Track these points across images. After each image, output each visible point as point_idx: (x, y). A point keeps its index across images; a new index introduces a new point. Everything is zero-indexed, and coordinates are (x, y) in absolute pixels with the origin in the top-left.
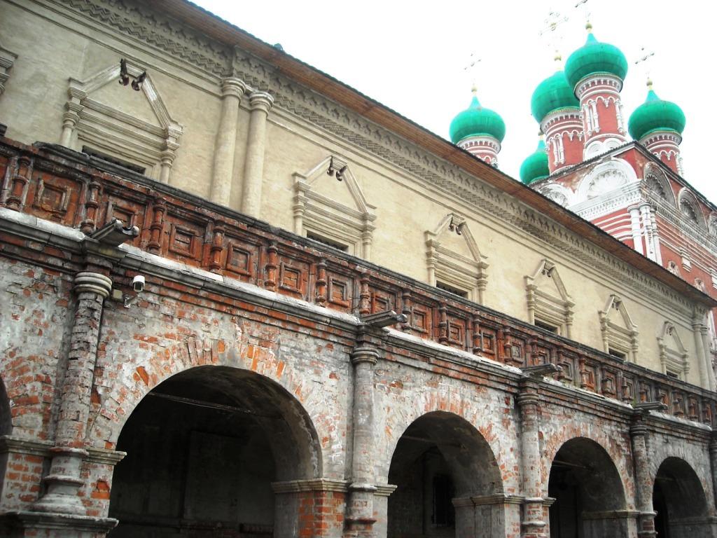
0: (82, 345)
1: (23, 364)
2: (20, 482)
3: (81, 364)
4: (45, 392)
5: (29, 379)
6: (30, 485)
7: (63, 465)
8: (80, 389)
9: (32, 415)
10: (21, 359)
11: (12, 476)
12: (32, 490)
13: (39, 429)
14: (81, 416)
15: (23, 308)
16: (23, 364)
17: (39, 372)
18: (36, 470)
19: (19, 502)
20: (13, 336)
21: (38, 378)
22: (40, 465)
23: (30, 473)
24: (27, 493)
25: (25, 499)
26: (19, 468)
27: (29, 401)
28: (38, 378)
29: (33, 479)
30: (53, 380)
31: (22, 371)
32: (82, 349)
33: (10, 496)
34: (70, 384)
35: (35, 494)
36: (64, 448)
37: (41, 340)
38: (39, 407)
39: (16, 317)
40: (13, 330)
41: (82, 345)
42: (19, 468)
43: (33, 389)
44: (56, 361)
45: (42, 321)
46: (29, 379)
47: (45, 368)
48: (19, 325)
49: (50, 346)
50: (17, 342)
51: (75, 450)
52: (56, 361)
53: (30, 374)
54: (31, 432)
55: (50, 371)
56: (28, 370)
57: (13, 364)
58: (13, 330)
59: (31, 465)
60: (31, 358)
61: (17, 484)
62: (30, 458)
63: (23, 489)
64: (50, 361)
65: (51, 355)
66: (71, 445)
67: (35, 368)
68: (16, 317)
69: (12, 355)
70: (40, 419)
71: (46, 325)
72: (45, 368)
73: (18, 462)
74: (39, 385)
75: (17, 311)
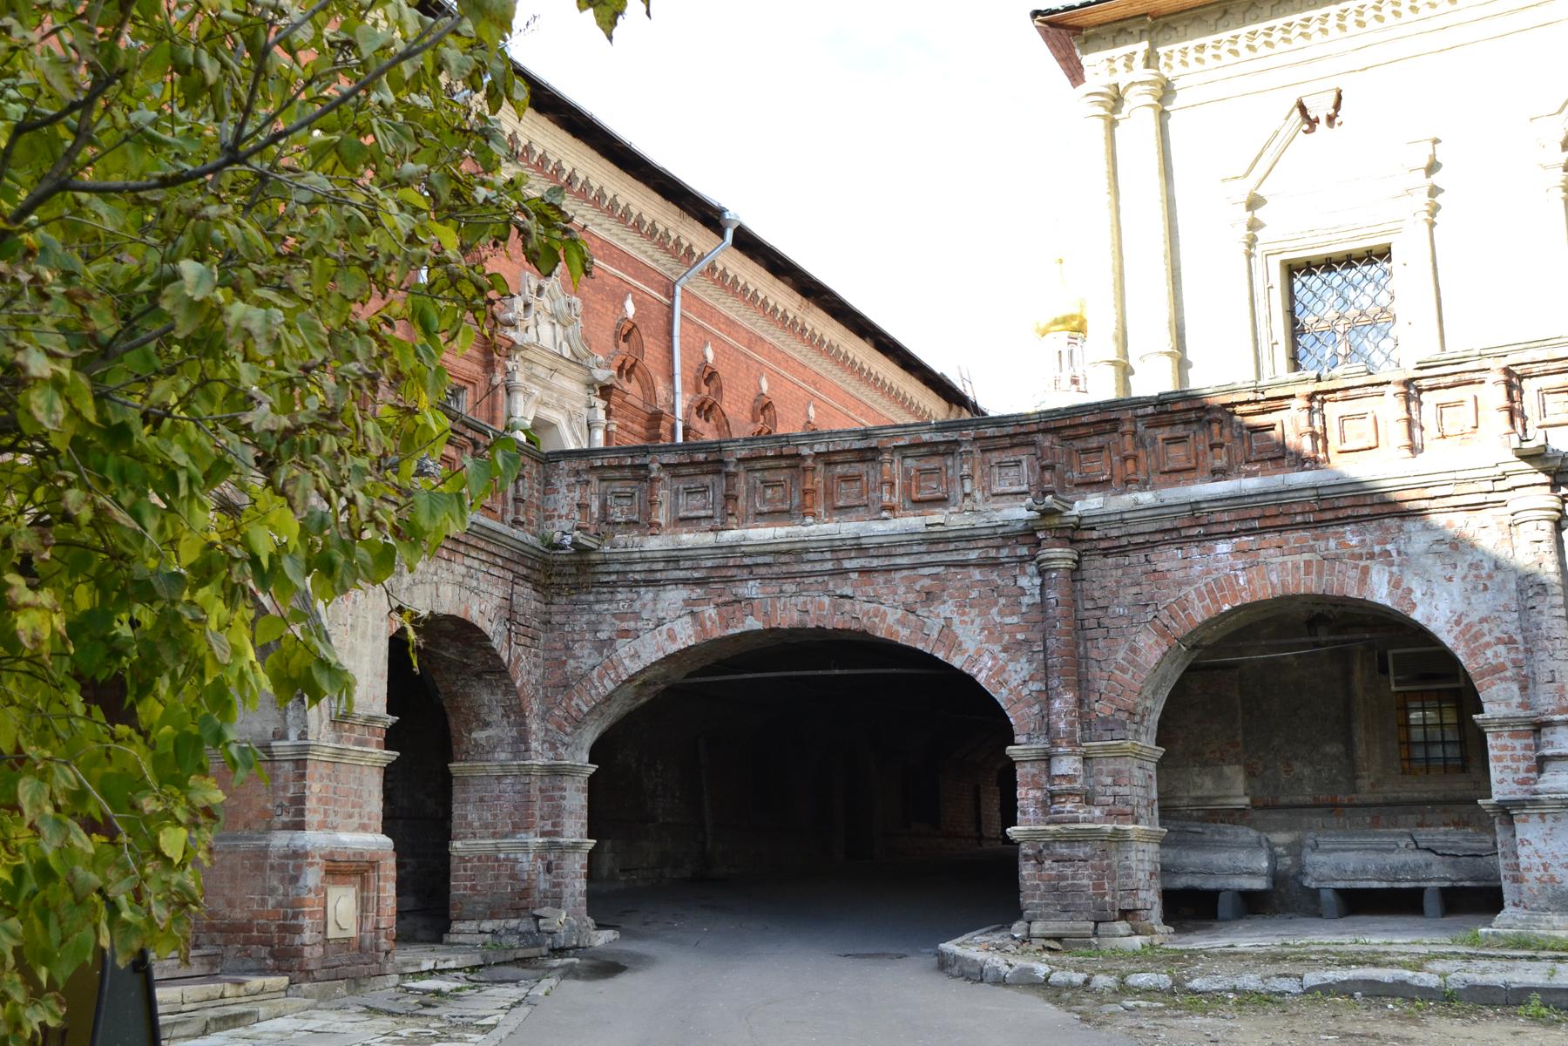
0: (1536, 589)
1: (1475, 629)
2: (1510, 764)
3: (1540, 613)
4: (1513, 655)
5: (1488, 645)
6: (1523, 765)
7: (1550, 738)
8: (1546, 643)
9: (1504, 685)
10: (1470, 626)
11: (1499, 759)
12: (1528, 770)
13: (1517, 699)
14: (1557, 675)
15: (1455, 566)
16: (1475, 629)
17: (1497, 633)
18: (1527, 747)
19: (1515, 786)
20: (1453, 601)
21: (1499, 641)
22: (1531, 741)
23: (1519, 752)
24: (1522, 775)
25: (1523, 782)
26: (1505, 748)
27: (1497, 669)
28: (1499, 641)
29: (1525, 758)
30: (1519, 638)
31: (1476, 637)
32: (1537, 594)
33: (1502, 781)
34: (1536, 638)
35: (1533, 775)
36: (1544, 718)
37: (1488, 595)
38: (1508, 674)
39: (1450, 579)
40: (1451, 595)
41: (1536, 589)
42: (1505, 748)
43: (1496, 655)
44: (1516, 615)
45: (1483, 573)
46: (1488, 645)
47: (1503, 626)
48: (1456, 587)
49: (1503, 599)
50: (1460, 607)
51: (1557, 718)
52: (1516, 615)
53: (1487, 639)
54: (1508, 705)
55: (1512, 628)
56: (1483, 635)
57: (1463, 633)
58: (1451, 595)
59: (1519, 743)
60: (1483, 620)
61: (1506, 767)
62: (1515, 735)
63: (1516, 771)
64: (1506, 617)
65: (1507, 609)
66: (1553, 713)
67: (1490, 631)
68: (1450, 579)
69: (1458, 623)
70: (1515, 687)
71: (1490, 577)
72: (1503, 626)
73: (1500, 742)
74: (1501, 649)
75: (1449, 572)
